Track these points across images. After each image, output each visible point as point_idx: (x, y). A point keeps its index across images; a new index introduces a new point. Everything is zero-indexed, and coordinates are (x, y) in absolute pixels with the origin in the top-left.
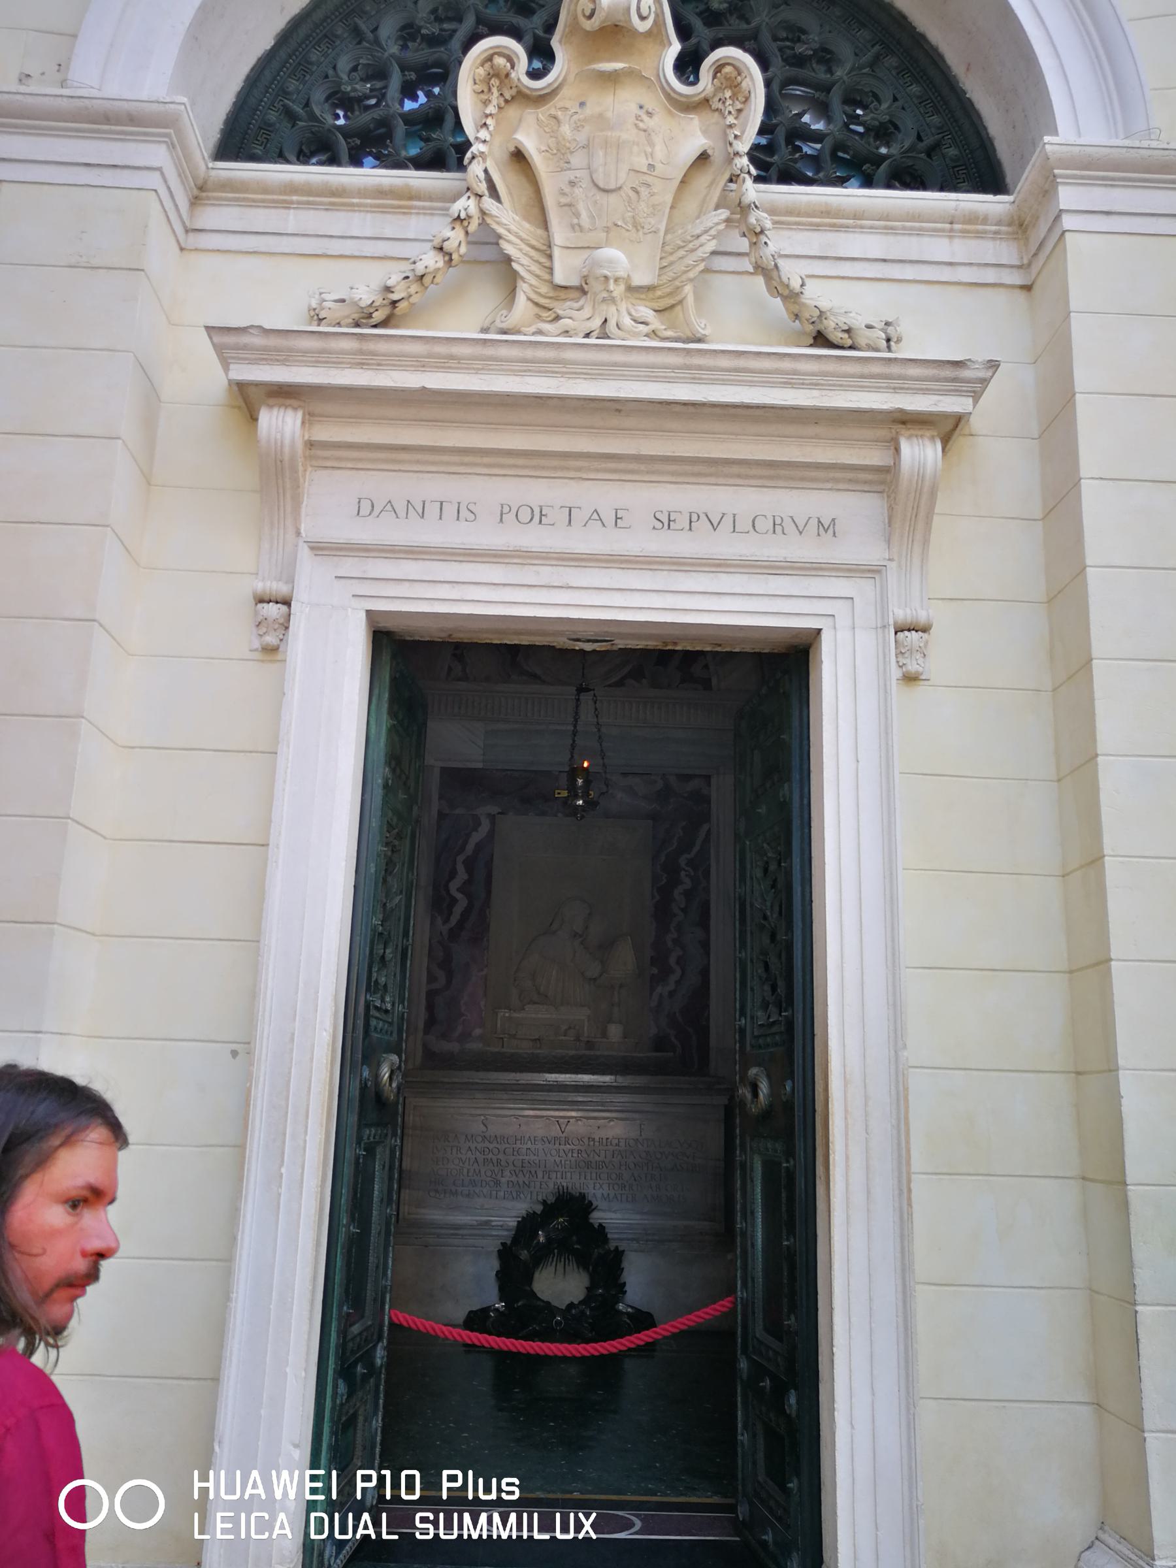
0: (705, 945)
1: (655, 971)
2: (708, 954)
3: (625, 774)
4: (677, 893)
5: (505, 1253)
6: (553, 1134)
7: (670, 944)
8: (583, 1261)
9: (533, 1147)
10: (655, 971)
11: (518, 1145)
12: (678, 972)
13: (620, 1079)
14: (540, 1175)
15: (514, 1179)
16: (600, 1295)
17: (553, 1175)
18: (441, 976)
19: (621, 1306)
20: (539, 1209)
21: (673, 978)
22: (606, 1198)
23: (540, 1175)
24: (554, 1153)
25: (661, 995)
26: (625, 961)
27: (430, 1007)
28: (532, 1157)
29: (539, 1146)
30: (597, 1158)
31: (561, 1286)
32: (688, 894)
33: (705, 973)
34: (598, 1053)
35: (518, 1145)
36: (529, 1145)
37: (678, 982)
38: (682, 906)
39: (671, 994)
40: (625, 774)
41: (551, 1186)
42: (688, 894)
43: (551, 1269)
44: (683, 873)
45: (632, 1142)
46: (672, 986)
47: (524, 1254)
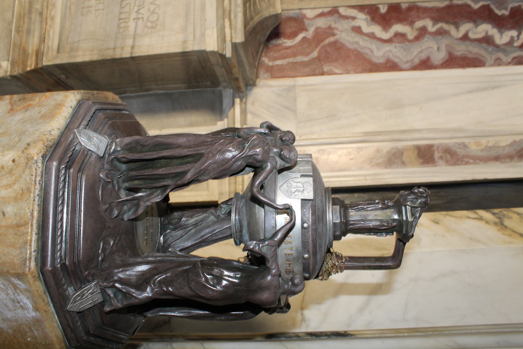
0: (425, 64)
1: (383, 10)
2: (415, 68)
4: (485, 29)
7: (419, 24)
10: (383, 10)
12: (386, 36)
21: (377, 30)
25: (354, 18)
32: (487, 40)
33: (391, 66)
37: (372, 36)
38: (471, 35)
39: (357, 30)
42: (487, 40)
44: (514, 33)
46: (366, 28)
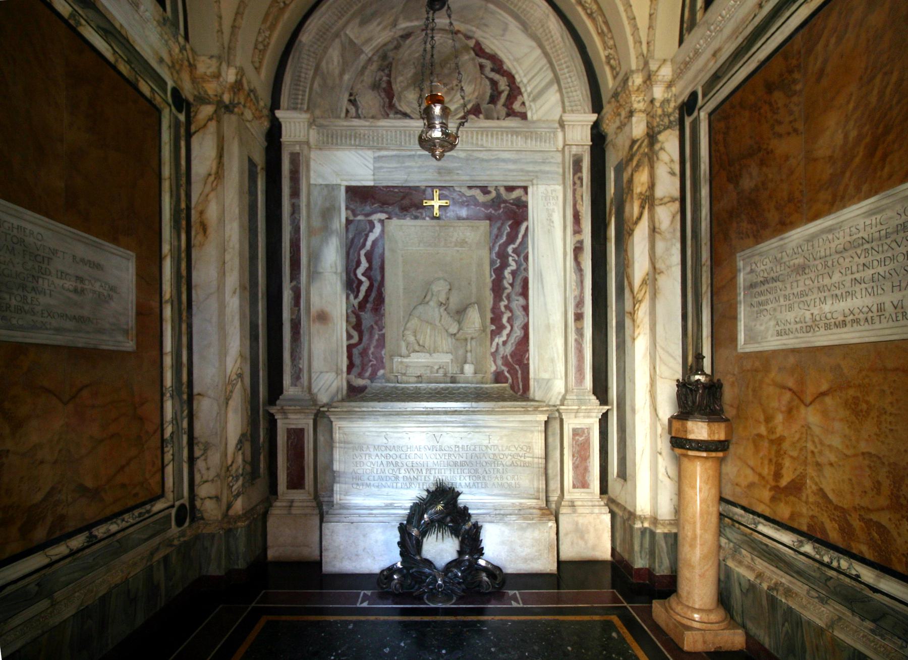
3: (470, 187)
5: (402, 529)
6: (432, 444)
8: (455, 532)
9: (419, 453)
11: (409, 452)
13: (474, 404)
14: (424, 471)
15: (407, 475)
16: (468, 560)
17: (433, 472)
18: (355, 334)
19: (482, 562)
20: (424, 494)
22: (468, 486)
23: (424, 471)
24: (433, 456)
26: (475, 320)
27: (350, 357)
28: (418, 460)
29: (423, 452)
30: (461, 459)
31: (441, 549)
34: (459, 385)
35: (409, 452)
36: (416, 452)
40: (470, 187)
41: (432, 478)
43: (434, 536)
45: (484, 448)
47: (415, 532)
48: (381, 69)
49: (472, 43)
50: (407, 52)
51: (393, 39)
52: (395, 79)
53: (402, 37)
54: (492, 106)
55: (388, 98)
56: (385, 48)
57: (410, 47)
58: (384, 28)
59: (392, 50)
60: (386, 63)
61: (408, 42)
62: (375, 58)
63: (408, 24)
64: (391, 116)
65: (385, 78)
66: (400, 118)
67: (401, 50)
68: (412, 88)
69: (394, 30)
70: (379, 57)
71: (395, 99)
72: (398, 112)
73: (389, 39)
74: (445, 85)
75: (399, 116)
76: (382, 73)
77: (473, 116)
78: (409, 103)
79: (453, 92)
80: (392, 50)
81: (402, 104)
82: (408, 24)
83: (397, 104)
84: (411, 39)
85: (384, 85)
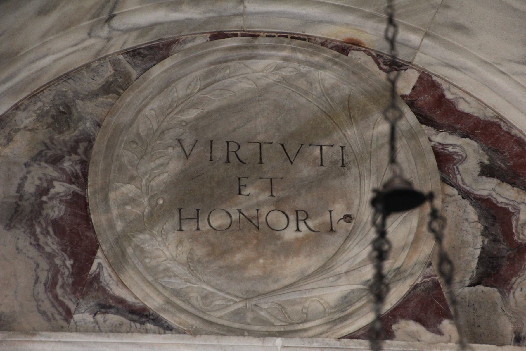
48: (47, 155)
49: (406, 83)
50: (155, 104)
51: (101, 58)
52: (105, 189)
53: (133, 53)
54: (493, 292)
55: (73, 255)
56: (64, 87)
57: (168, 83)
58: (65, 27)
59: (94, 95)
60: (68, 136)
61: (158, 71)
62: (25, 119)
63: (161, 15)
64: (82, 317)
65: (59, 188)
66: (115, 330)
67: (131, 98)
68: (173, 221)
69: (104, 32)
70: (41, 116)
71: (99, 259)
72: (108, 304)
73: (80, 59)
74: (302, 215)
75: (113, 318)
76: (51, 171)
77: (413, 326)
78: (155, 275)
79: (334, 242)
80: (94, 95)
81: (130, 276)
82: (161, 15)
83: (107, 277)
84: (168, 63)
85: (56, 210)
